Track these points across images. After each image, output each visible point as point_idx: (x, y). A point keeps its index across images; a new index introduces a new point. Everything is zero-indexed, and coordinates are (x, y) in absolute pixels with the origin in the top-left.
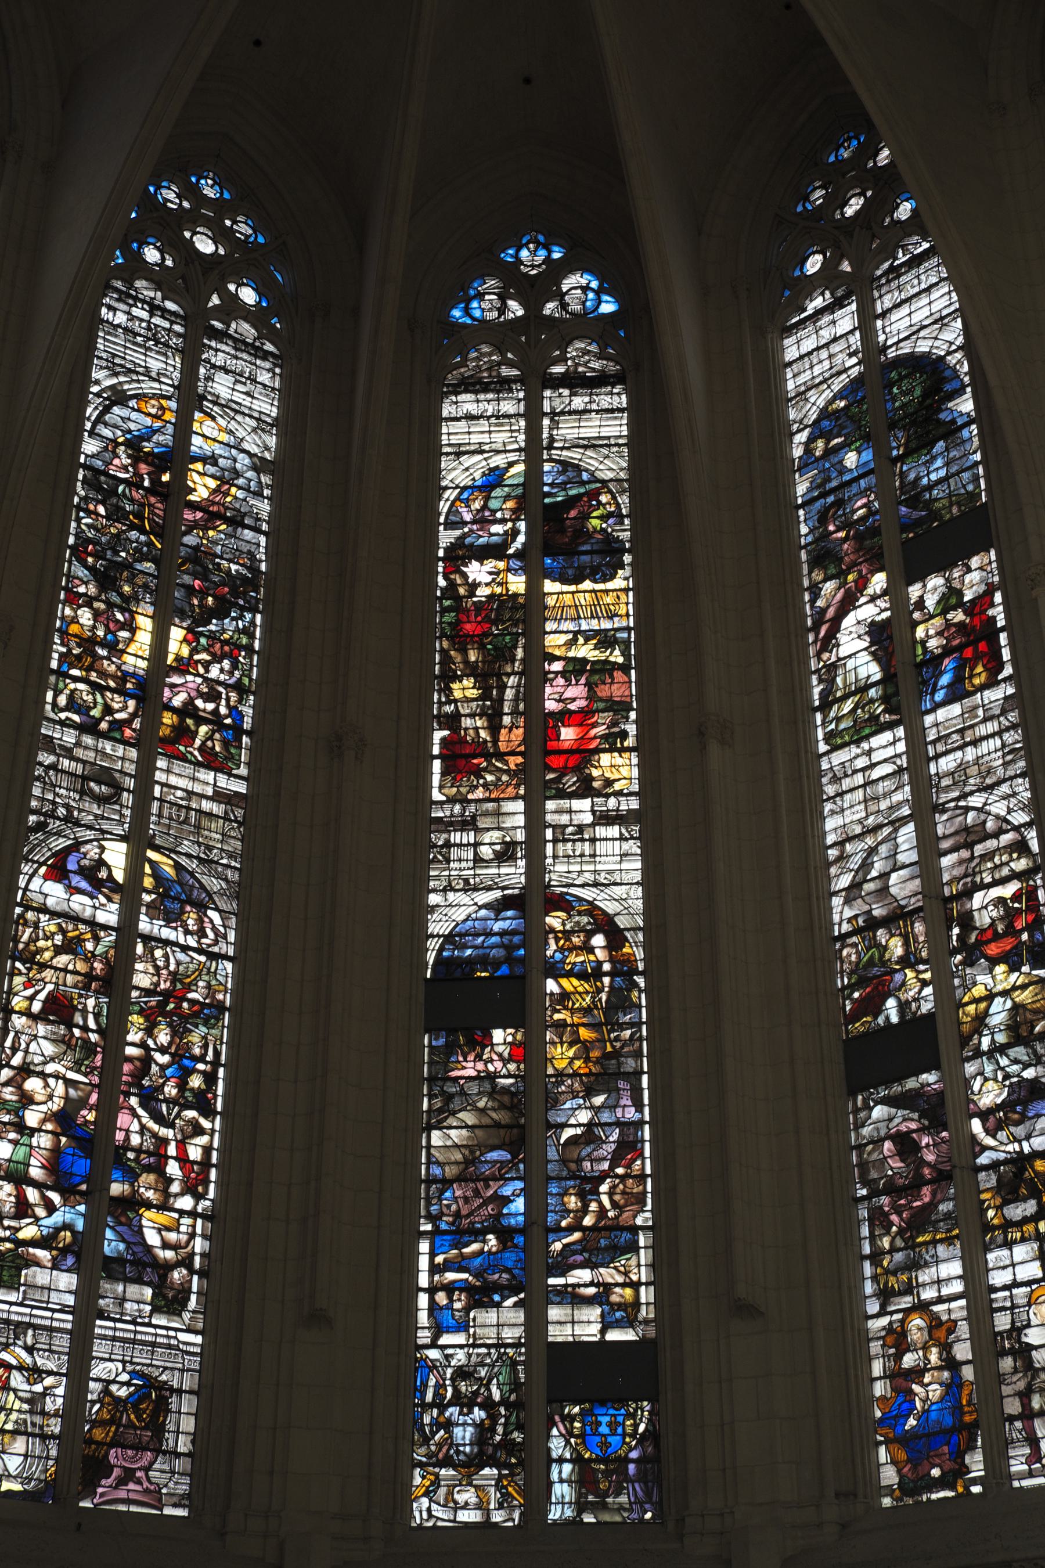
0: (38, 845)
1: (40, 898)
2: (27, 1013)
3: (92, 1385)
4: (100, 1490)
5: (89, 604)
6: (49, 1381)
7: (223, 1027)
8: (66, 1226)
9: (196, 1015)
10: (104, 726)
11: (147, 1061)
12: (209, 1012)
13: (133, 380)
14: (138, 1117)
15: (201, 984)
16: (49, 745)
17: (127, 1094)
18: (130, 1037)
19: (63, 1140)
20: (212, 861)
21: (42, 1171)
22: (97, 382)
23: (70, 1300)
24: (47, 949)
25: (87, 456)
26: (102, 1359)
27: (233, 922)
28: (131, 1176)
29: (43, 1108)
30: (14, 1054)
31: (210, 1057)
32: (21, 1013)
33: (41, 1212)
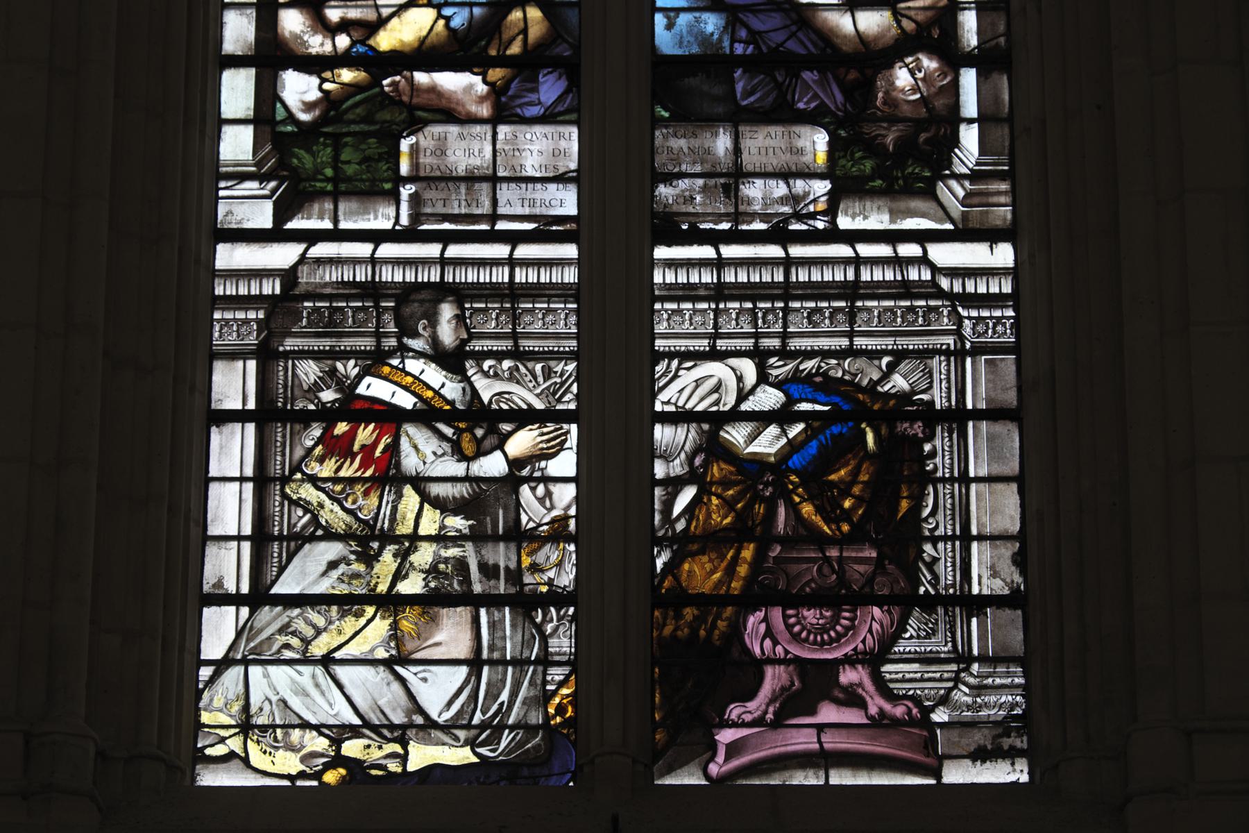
3: (662, 434)
4: (726, 736)
6: (522, 442)
23: (565, 201)
26: (685, 356)
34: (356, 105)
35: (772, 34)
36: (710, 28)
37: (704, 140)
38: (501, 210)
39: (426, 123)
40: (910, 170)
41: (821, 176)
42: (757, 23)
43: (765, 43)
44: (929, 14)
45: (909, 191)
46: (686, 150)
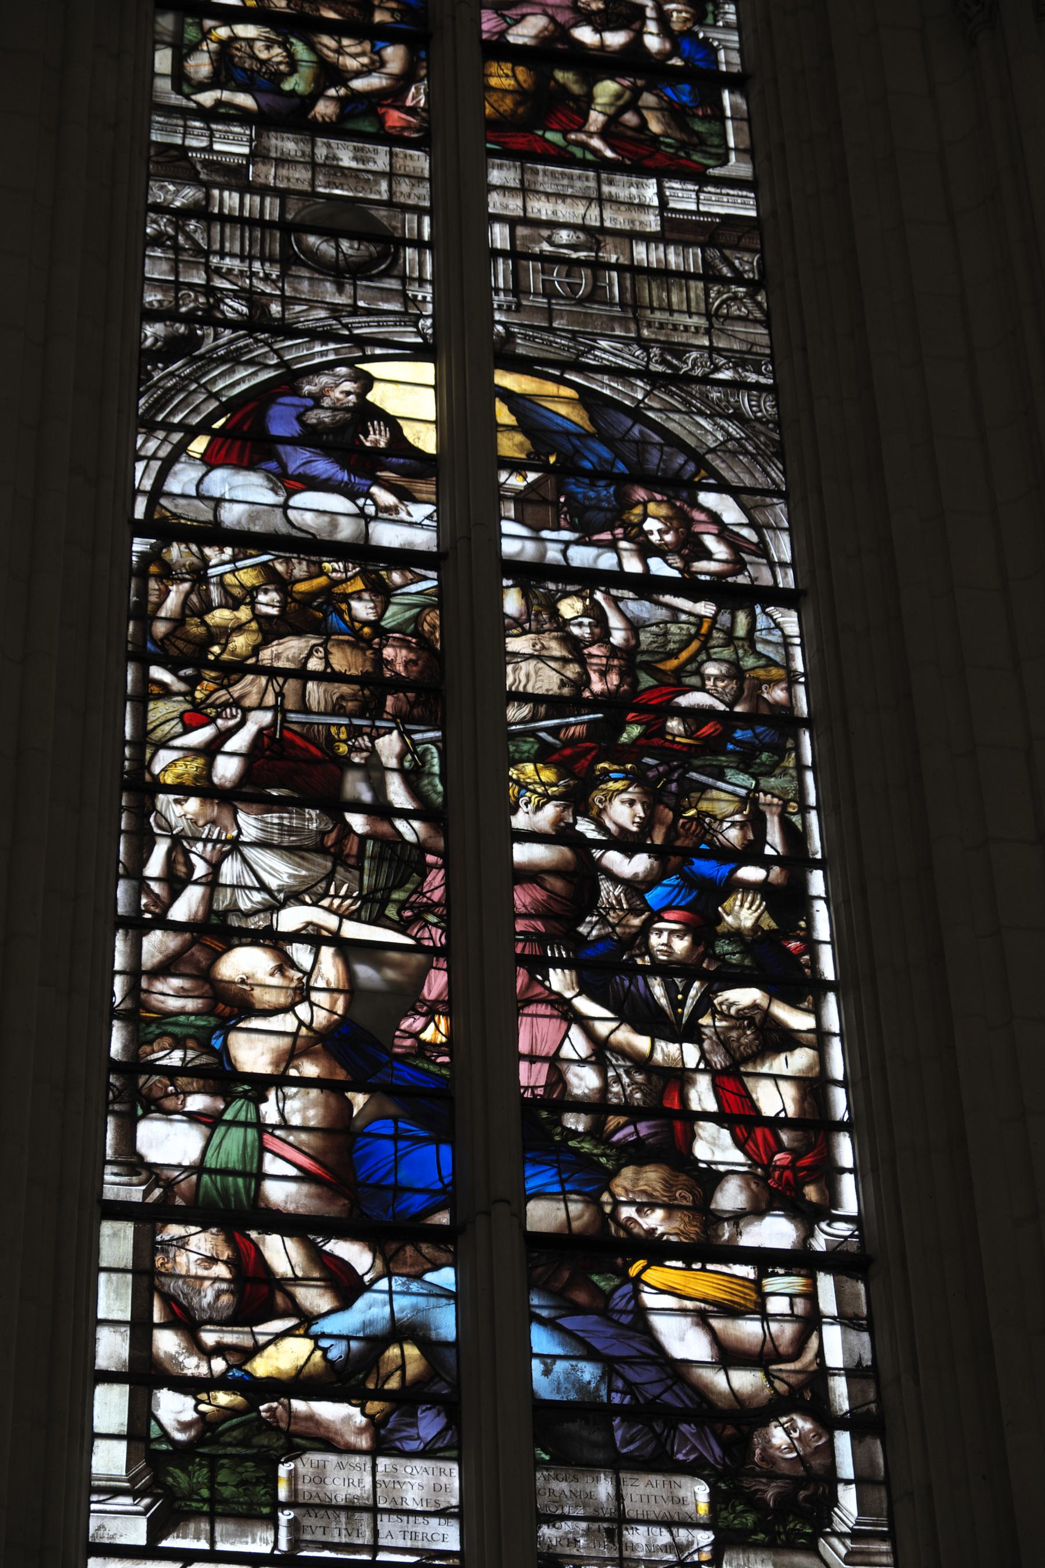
0: (177, 389)
1: (203, 512)
2: (202, 787)
7: (801, 768)
8: (400, 1331)
9: (712, 746)
10: (324, 109)
11: (582, 874)
12: (753, 735)
14: (584, 1023)
15: (712, 669)
16: (178, 164)
17: (540, 966)
18: (520, 821)
19: (359, 1100)
20: (689, 379)
21: (305, 1188)
24: (240, 628)
27: (780, 513)
28: (586, 1175)
29: (286, 1023)
30: (175, 894)
31: (774, 841)
32: (182, 791)
33: (314, 1298)
34: (233, 1428)
35: (648, 1386)
36: (587, 1377)
37: (585, 1484)
38: (382, 1542)
39: (305, 1450)
40: (791, 1526)
41: (704, 1527)
42: (632, 1375)
43: (641, 1394)
44: (801, 1377)
45: (791, 1547)
46: (567, 1493)
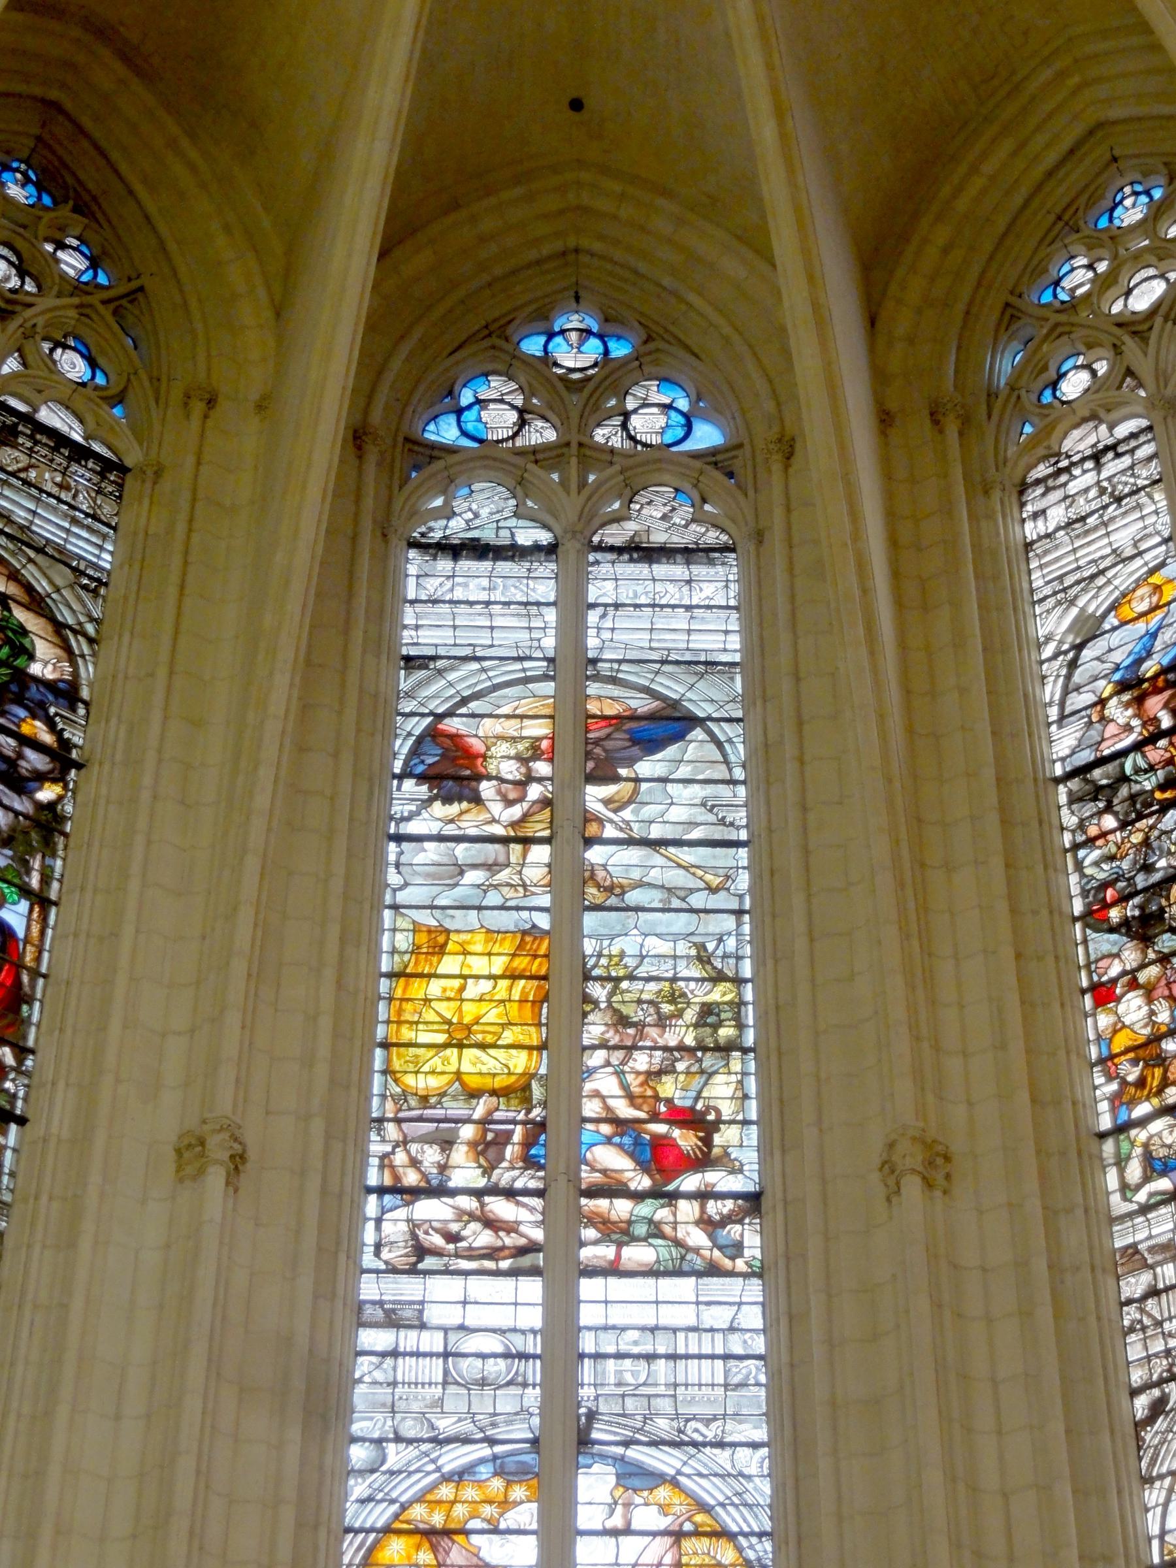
0: (1162, 1443)
5: (1133, 985)
13: (1100, 588)
22: (1048, 639)
25: (1063, 760)
